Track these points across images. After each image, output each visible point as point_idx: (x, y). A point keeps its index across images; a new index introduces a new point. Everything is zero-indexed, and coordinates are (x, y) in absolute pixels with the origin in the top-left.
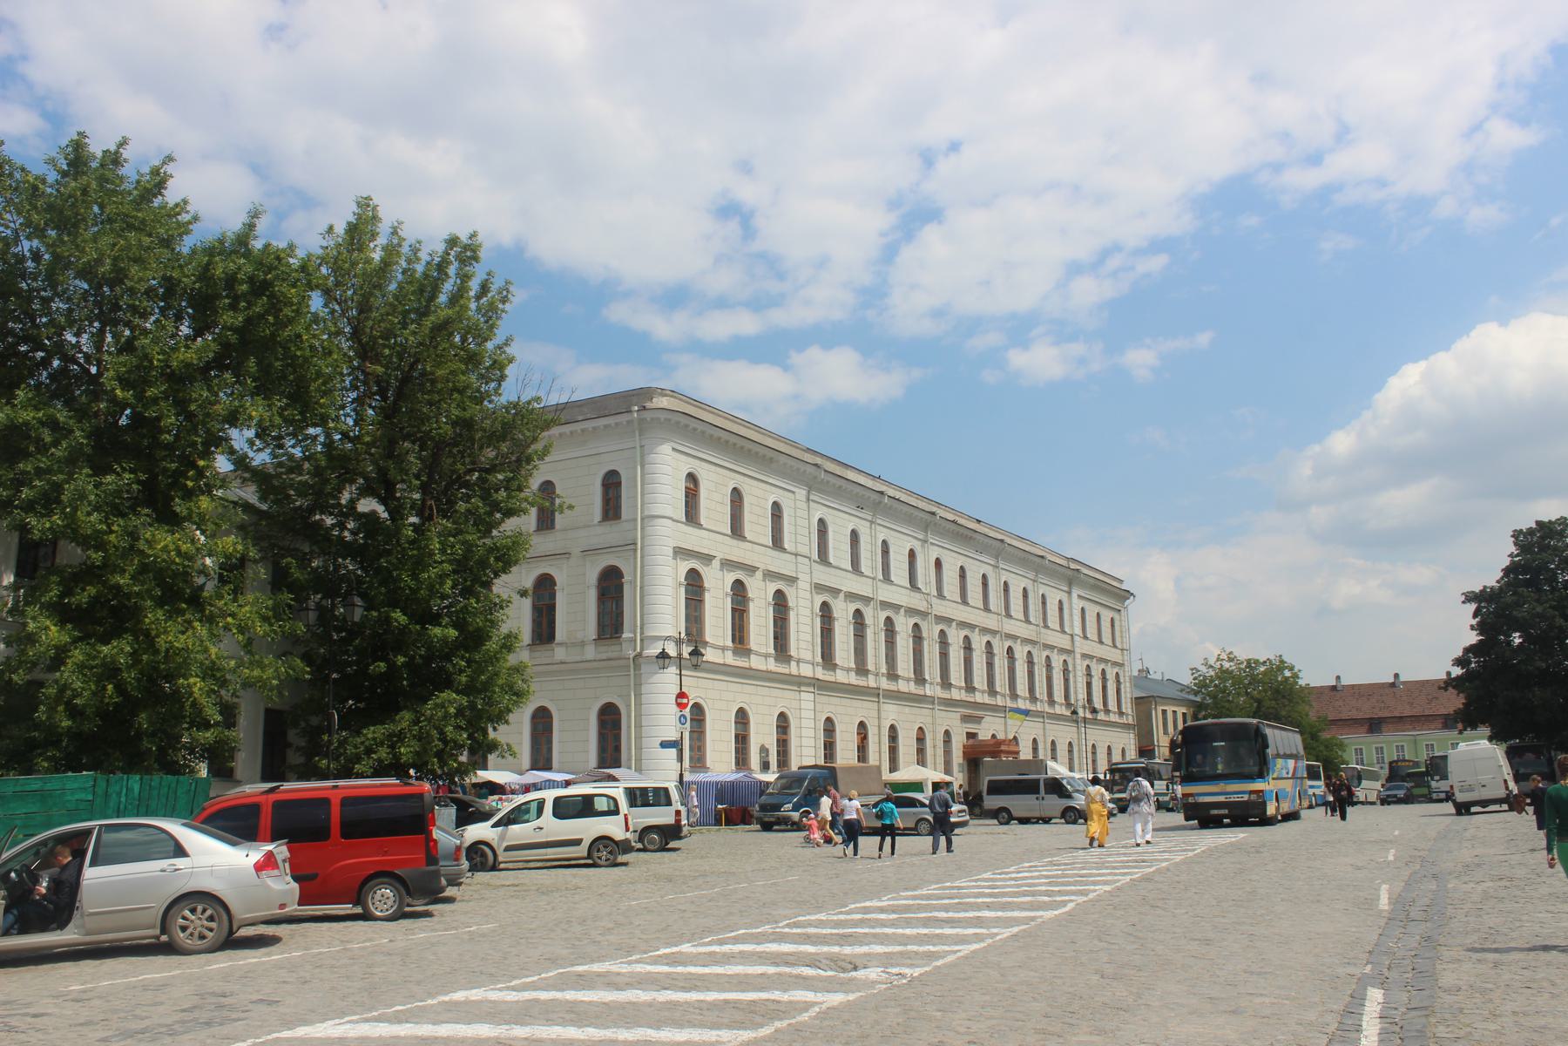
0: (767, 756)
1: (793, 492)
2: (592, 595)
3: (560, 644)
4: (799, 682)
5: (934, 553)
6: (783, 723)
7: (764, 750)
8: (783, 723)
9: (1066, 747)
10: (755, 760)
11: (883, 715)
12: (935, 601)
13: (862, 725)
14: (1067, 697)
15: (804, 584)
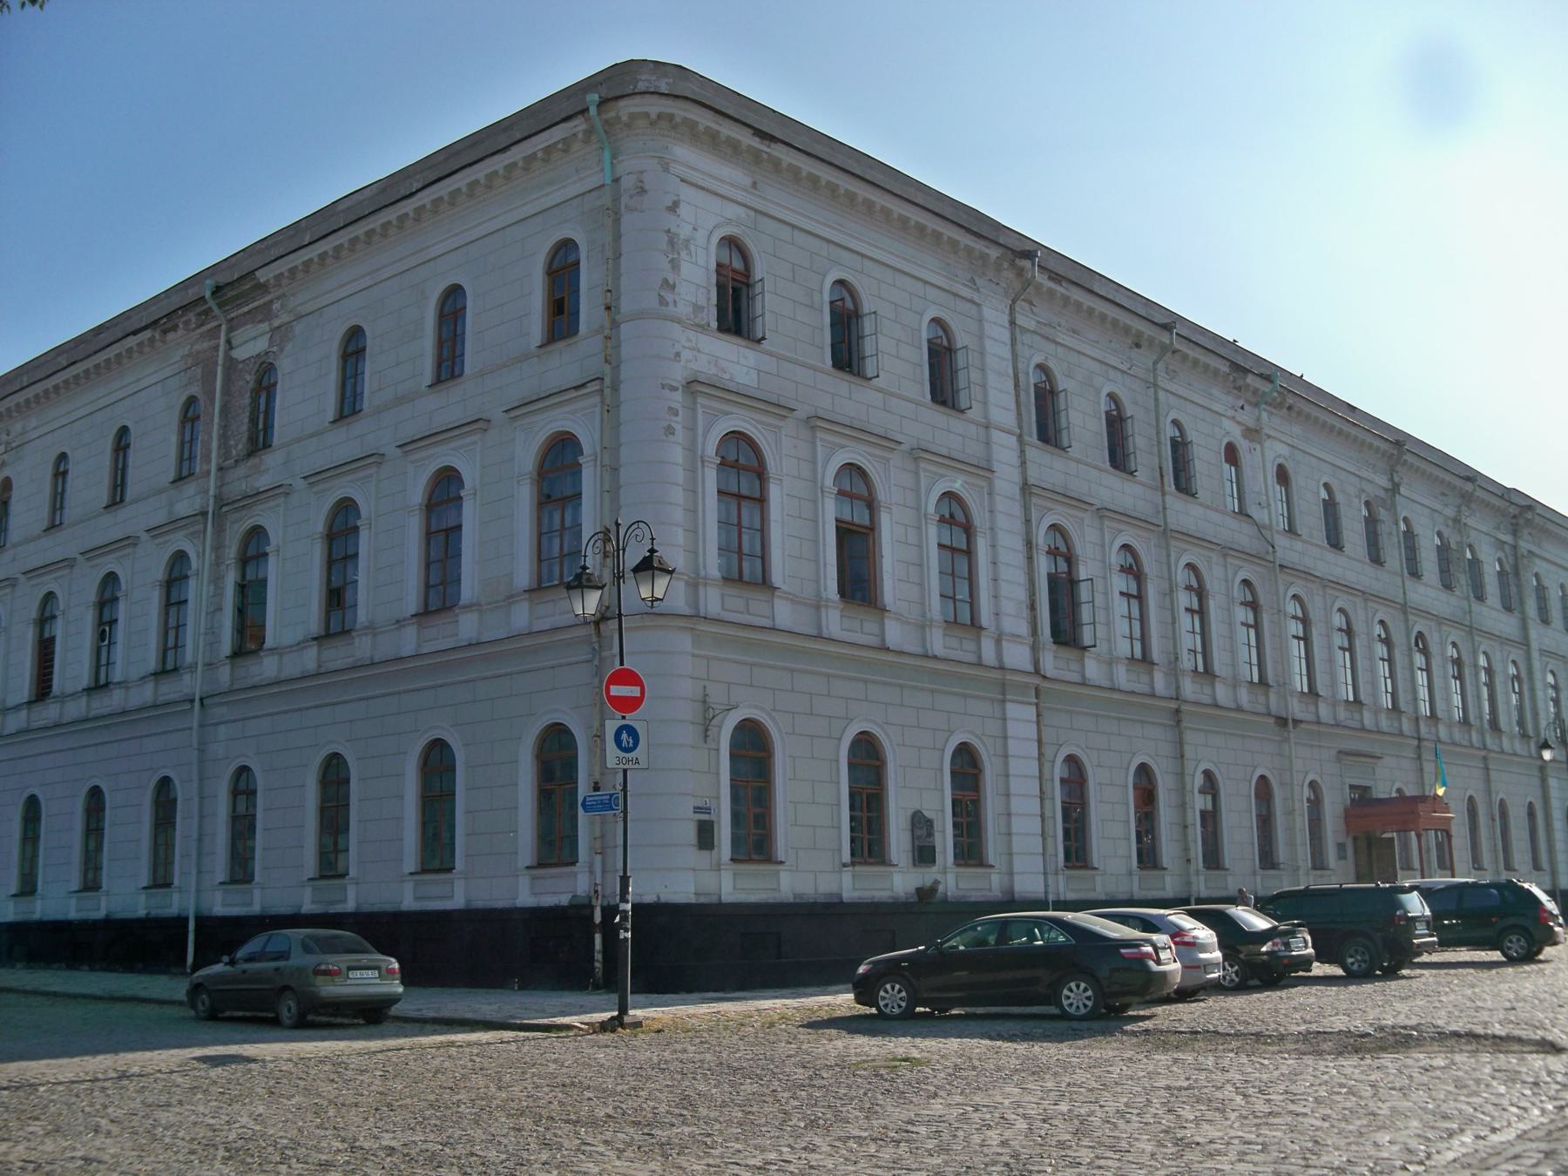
0: (930, 834)
1: (978, 305)
2: (525, 496)
3: (469, 607)
4: (1002, 685)
5: (1275, 451)
6: (967, 768)
7: (920, 824)
8: (967, 768)
9: (1523, 812)
10: (898, 839)
11: (1189, 751)
12: (1282, 542)
13: (1144, 770)
14: (1521, 723)
15: (1006, 480)
